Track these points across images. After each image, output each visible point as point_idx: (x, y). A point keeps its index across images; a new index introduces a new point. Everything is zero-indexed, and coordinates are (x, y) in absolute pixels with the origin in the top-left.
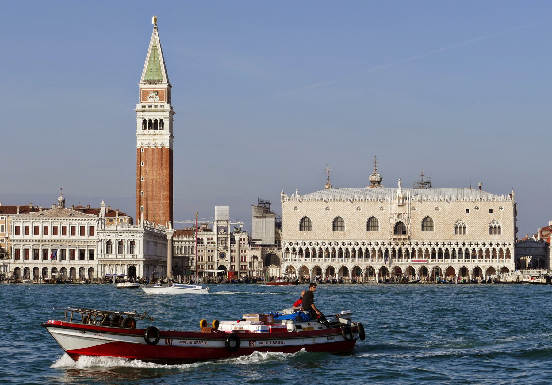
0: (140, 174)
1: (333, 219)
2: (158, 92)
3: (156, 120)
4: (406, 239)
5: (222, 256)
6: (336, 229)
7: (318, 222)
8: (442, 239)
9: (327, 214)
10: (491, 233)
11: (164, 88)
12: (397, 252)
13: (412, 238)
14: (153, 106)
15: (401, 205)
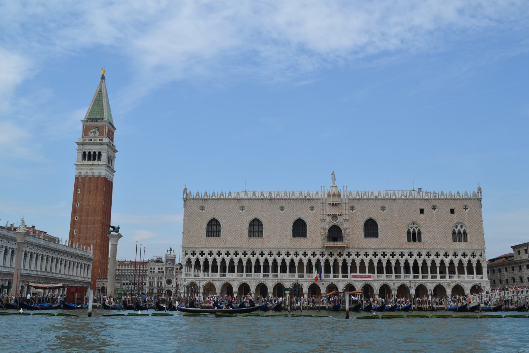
0: (76, 200)
1: (247, 222)
2: (98, 128)
3: (95, 153)
4: (344, 247)
5: (169, 282)
6: (252, 235)
7: (230, 226)
8: (391, 249)
9: (241, 216)
10: (454, 241)
11: (104, 125)
12: (331, 264)
13: (351, 247)
14: (93, 140)
15: (336, 204)
